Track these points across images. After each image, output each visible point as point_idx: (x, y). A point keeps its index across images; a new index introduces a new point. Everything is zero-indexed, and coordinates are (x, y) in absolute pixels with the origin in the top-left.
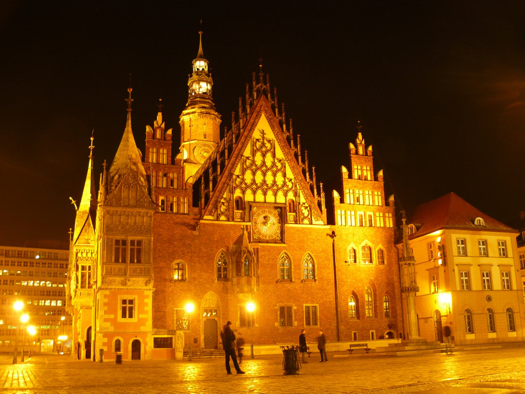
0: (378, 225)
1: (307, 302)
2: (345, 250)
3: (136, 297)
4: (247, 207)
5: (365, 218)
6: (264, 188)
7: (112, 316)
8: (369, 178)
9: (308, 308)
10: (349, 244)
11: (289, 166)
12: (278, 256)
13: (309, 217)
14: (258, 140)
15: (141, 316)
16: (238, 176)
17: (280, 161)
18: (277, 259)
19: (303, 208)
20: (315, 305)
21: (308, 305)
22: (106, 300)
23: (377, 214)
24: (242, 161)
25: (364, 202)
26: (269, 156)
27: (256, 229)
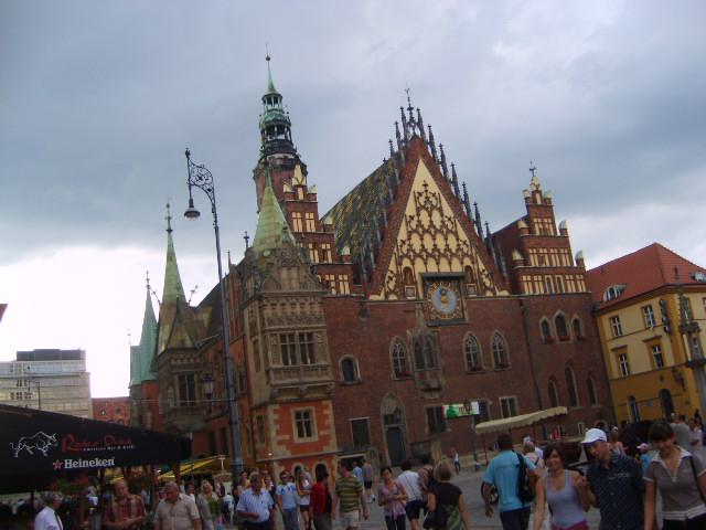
0: (570, 291)
1: (503, 395)
3: (313, 408)
4: (418, 279)
6: (436, 255)
7: (287, 437)
9: (503, 401)
14: (420, 194)
15: (322, 433)
16: (403, 242)
17: (450, 219)
19: (483, 276)
22: (277, 417)
23: (567, 277)
24: (404, 223)
26: (436, 214)
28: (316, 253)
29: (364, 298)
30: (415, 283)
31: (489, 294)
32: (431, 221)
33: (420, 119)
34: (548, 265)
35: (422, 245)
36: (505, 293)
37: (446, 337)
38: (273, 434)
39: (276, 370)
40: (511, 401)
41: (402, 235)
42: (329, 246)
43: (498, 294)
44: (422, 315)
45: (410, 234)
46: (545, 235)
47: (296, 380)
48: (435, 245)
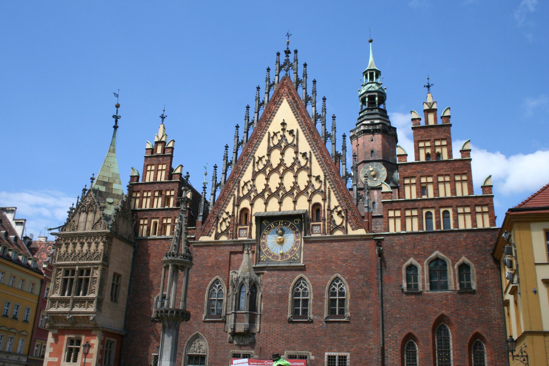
0: (461, 227)
2: (400, 268)
5: (438, 217)
6: (280, 194)
7: (56, 359)
8: (445, 157)
9: (331, 359)
10: (406, 261)
11: (317, 159)
12: (291, 282)
13: (344, 225)
14: (275, 134)
17: (304, 155)
18: (289, 286)
20: (343, 354)
21: (332, 354)
25: (435, 194)
26: (290, 153)
27: (265, 247)
28: (160, 199)
29: (194, 239)
30: (251, 224)
31: (338, 233)
32: (282, 160)
33: (296, 60)
34: (431, 195)
35: (267, 185)
36: (361, 232)
37: (269, 280)
38: (47, 355)
39: (53, 300)
40: (343, 359)
41: (247, 176)
42: (173, 193)
43: (351, 232)
44: (251, 255)
45: (255, 175)
46: (434, 159)
47: (67, 309)
48: (281, 184)
